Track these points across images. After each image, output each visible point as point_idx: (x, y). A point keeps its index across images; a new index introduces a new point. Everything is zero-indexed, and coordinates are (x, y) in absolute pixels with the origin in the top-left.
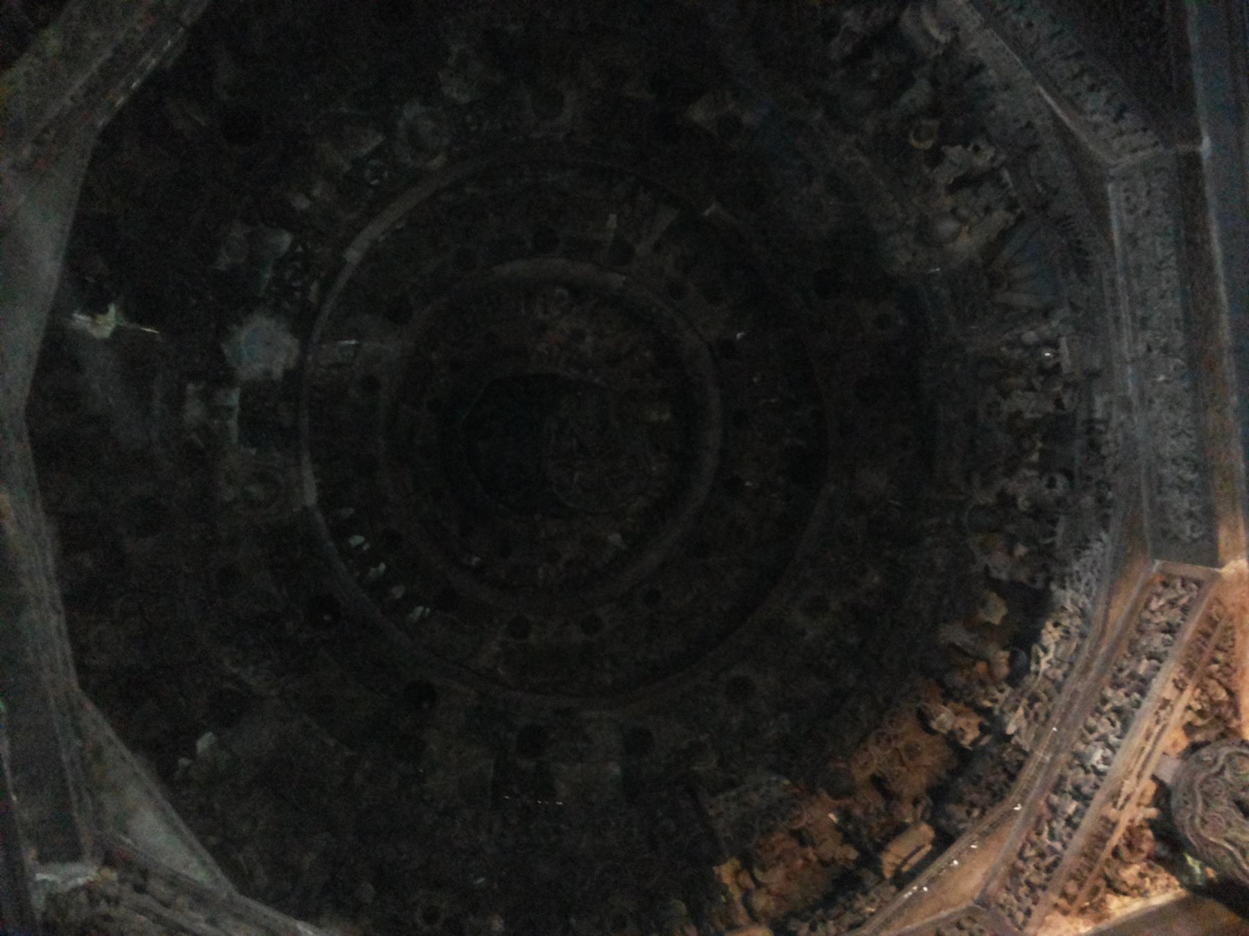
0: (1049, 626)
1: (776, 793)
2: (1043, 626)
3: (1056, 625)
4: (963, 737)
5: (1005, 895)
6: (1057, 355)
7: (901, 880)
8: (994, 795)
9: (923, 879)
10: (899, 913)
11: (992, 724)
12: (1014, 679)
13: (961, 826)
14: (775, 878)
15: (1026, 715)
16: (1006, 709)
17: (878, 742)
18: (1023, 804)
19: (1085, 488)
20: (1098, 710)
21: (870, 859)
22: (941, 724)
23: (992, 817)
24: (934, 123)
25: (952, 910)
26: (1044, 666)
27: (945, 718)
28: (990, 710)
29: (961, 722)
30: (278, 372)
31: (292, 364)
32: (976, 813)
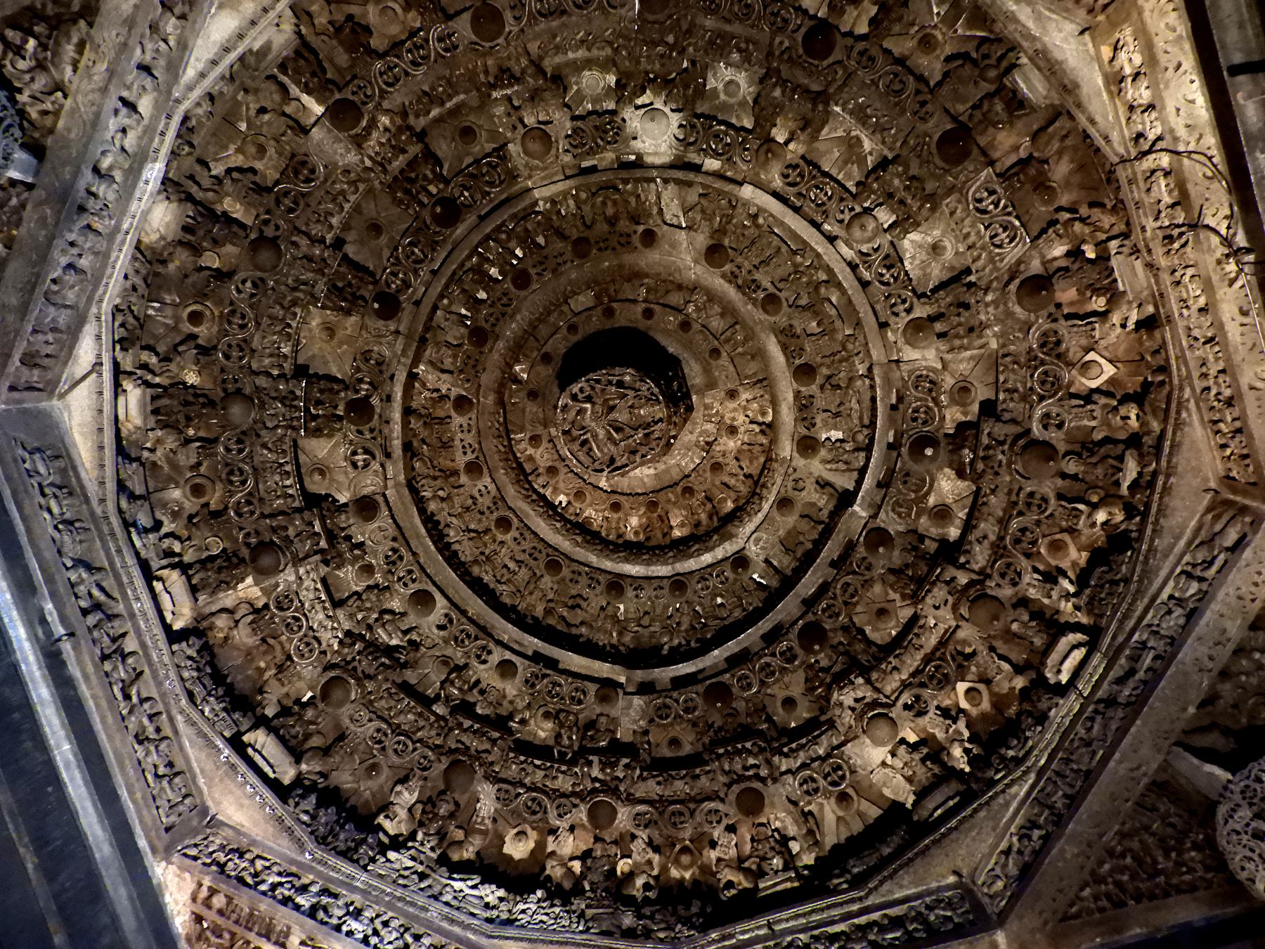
0: (501, 893)
1: (325, 636)
2: (499, 887)
3: (501, 899)
4: (387, 817)
5: (218, 842)
6: (776, 872)
7: (237, 744)
8: (324, 838)
9: (235, 759)
10: (201, 734)
11: (398, 843)
12: (443, 860)
13: (291, 802)
14: (244, 636)
15: (407, 869)
16: (412, 852)
17: (378, 730)
18: (314, 860)
19: (640, 917)
20: (407, 930)
21: (261, 722)
22: (399, 793)
23: (299, 831)
24: (986, 705)
25: (205, 789)
26: (458, 885)
27: (407, 797)
28: (414, 840)
29: (403, 814)
30: (637, 145)
31: (649, 160)
32: (305, 818)
